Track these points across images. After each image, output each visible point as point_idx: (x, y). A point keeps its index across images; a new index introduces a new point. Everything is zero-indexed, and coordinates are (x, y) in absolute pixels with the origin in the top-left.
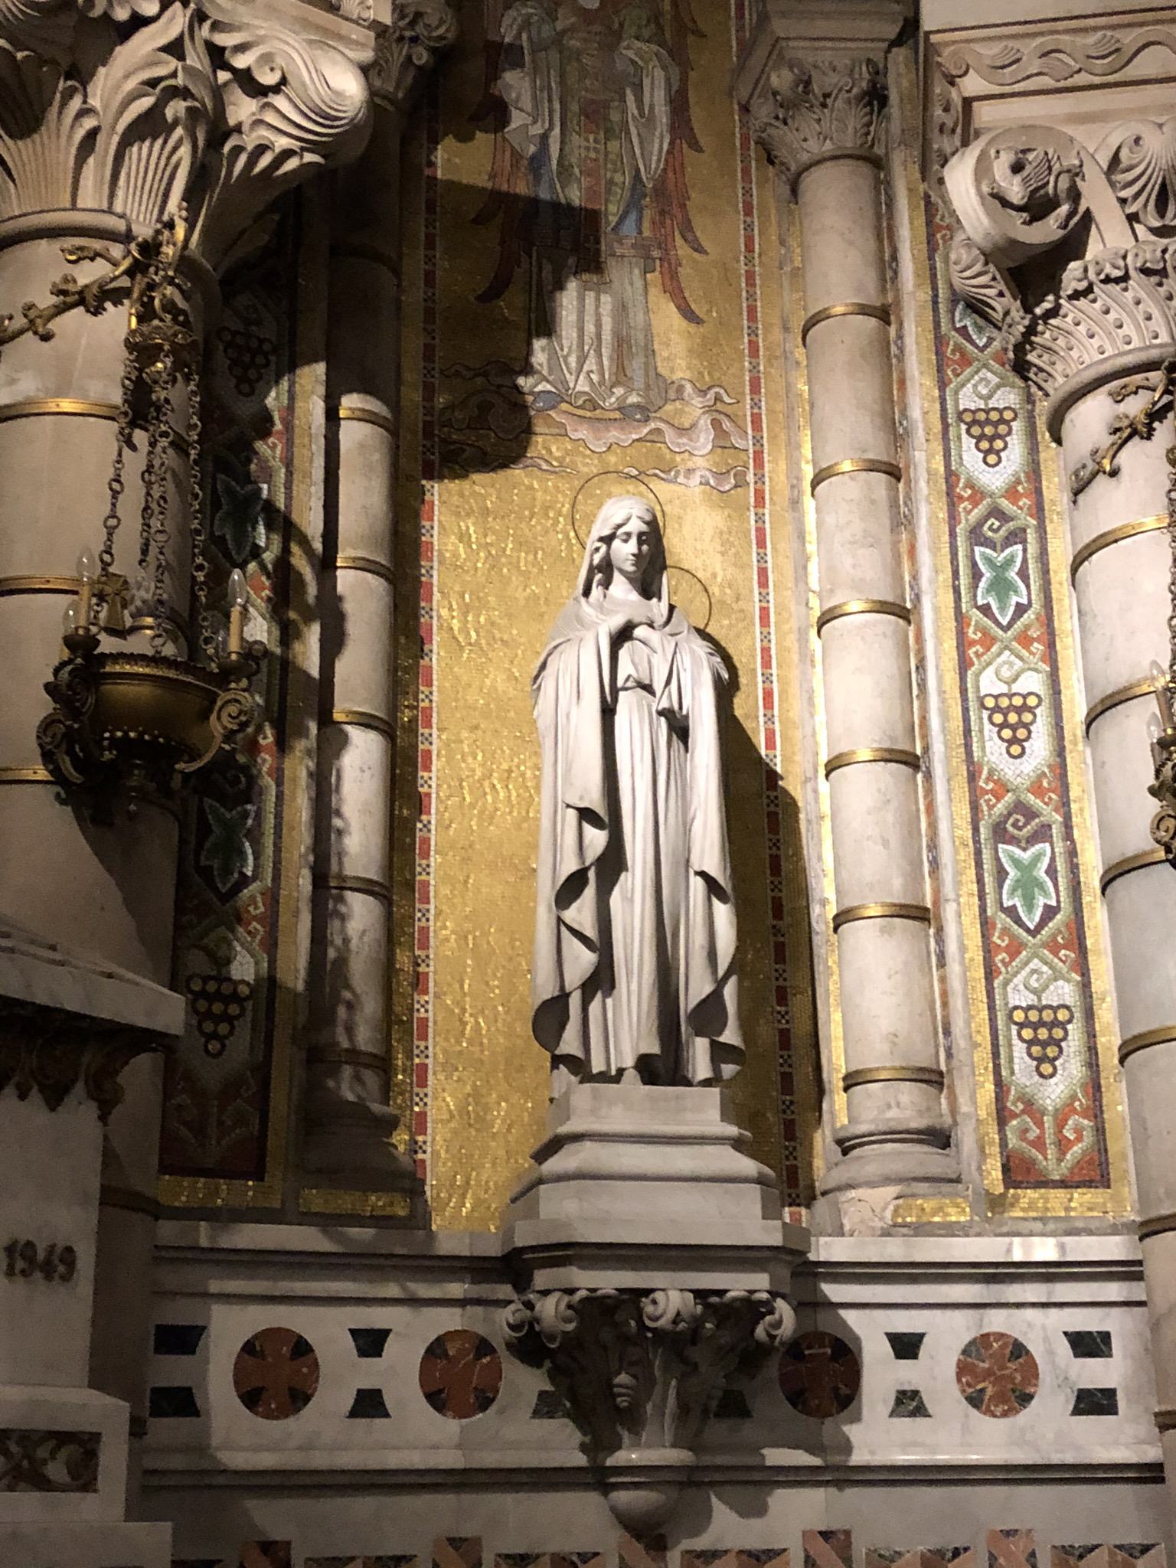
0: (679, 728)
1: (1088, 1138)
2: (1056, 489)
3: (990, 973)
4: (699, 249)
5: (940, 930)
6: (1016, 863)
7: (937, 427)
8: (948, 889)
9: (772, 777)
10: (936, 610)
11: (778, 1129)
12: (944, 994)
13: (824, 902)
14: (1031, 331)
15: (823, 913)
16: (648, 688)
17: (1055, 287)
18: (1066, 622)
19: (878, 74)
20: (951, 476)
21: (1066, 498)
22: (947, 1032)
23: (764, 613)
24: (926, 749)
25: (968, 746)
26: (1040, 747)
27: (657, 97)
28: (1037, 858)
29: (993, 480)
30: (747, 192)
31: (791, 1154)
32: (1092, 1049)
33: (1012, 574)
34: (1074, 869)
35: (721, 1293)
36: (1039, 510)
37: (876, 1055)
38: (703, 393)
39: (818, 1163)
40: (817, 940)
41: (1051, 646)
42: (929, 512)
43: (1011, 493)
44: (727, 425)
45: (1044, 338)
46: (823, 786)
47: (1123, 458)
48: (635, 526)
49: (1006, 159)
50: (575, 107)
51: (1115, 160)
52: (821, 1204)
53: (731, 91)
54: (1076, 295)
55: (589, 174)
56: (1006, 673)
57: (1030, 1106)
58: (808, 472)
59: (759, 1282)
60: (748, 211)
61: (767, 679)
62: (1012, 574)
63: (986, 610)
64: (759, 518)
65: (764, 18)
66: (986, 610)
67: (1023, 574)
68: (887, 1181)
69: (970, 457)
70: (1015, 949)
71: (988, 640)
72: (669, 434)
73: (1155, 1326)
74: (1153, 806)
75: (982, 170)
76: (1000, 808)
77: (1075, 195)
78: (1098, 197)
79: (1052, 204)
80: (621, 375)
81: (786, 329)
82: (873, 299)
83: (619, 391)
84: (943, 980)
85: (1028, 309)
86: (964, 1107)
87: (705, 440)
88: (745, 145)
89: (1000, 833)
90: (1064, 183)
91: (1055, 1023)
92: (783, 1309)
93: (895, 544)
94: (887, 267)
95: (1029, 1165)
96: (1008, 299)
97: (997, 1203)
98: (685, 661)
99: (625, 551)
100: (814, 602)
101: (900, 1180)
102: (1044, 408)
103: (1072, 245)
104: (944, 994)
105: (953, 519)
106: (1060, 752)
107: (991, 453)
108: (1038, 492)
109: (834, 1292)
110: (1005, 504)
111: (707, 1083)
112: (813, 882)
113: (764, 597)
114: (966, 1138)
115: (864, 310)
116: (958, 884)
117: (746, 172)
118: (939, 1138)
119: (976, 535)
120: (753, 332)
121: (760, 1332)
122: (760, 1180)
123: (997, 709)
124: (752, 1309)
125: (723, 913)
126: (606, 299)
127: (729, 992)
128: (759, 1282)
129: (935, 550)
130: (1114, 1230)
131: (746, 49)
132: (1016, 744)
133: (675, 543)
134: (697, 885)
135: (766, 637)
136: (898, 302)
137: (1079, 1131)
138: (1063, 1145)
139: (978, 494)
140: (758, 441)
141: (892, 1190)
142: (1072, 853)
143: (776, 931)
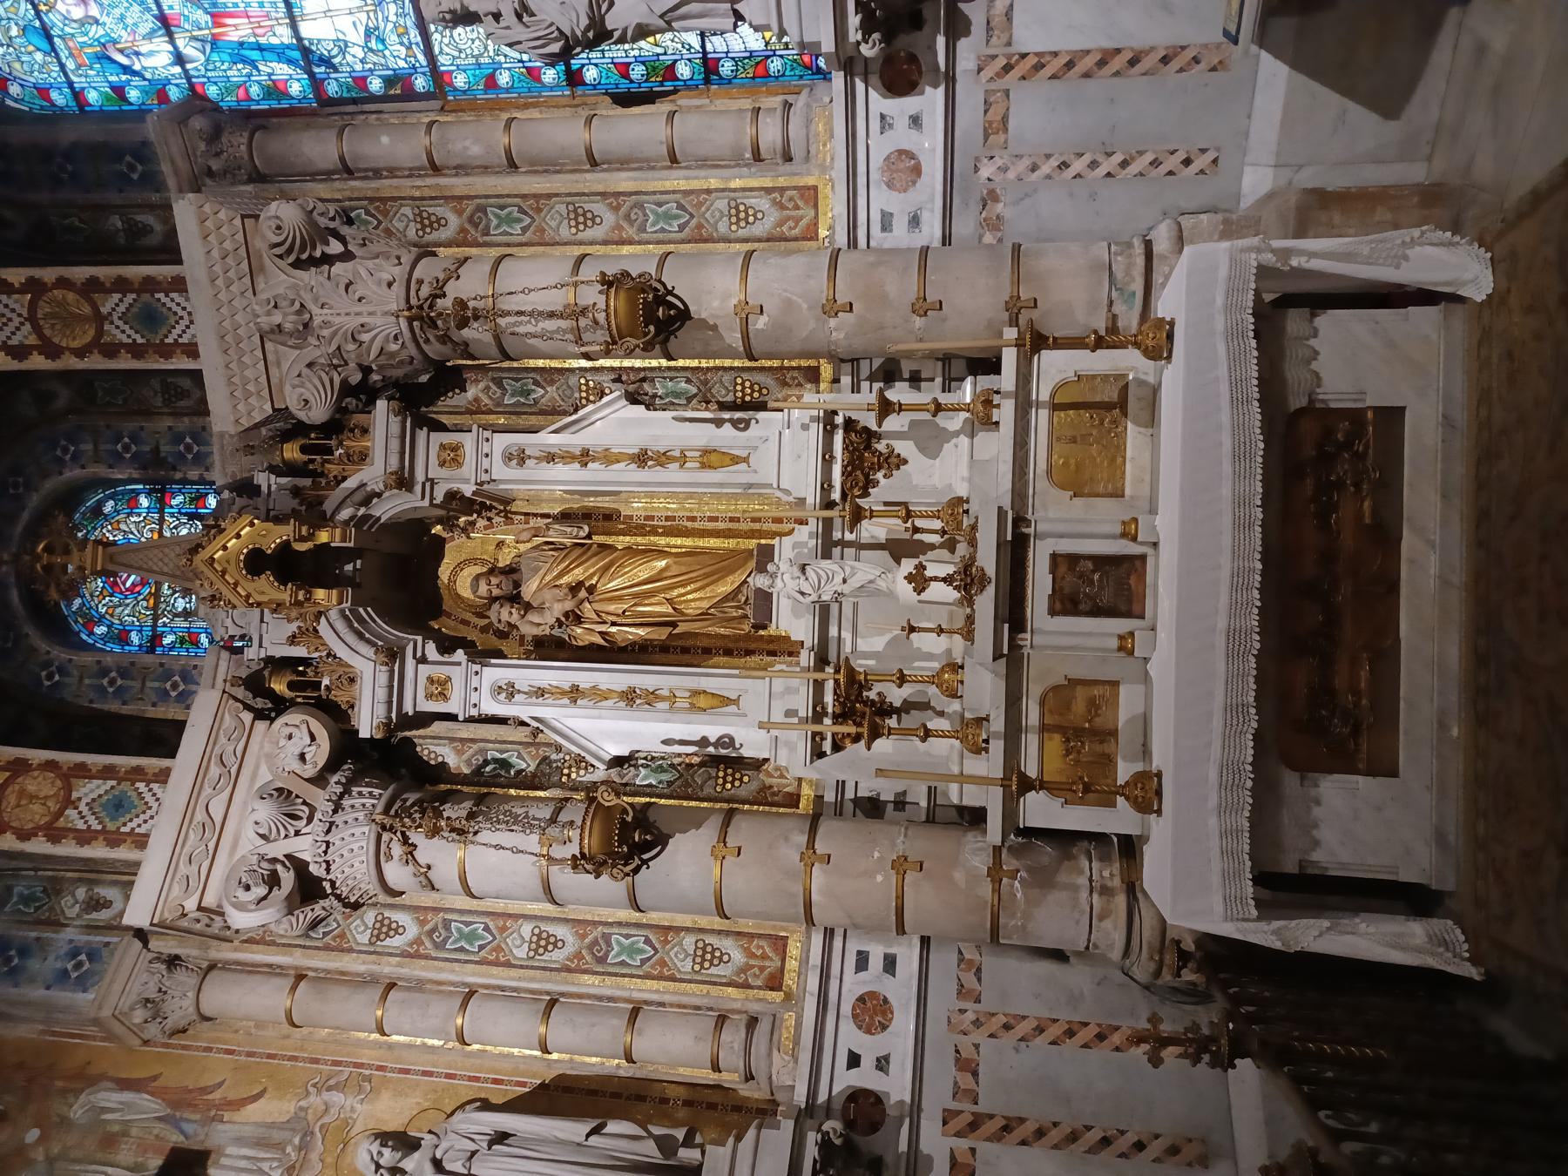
0: (501, 1137)
1: (763, 943)
2: (428, 899)
3: (673, 979)
4: (220, 1084)
5: (646, 1002)
6: (618, 954)
7: (373, 957)
8: (625, 994)
9: (543, 1086)
10: (474, 974)
11: (735, 1116)
12: (679, 1006)
13: (618, 1066)
14: (338, 897)
15: (626, 1070)
16: (474, 1153)
17: (321, 880)
18: (500, 906)
19: (158, 958)
20: (404, 954)
21: (434, 894)
22: (698, 1008)
23: (449, 1076)
24: (548, 993)
25: (551, 970)
26: (561, 931)
27: (110, 1098)
28: (618, 943)
29: (412, 931)
30: (198, 1048)
31: (749, 1110)
32: (720, 932)
33: (466, 930)
34: (628, 925)
35: (815, 1161)
36: (436, 910)
37: (704, 1052)
38: (308, 1094)
39: (756, 1095)
40: (638, 1075)
41: (510, 916)
42: (419, 970)
43: (422, 923)
44: (332, 1082)
45: (344, 891)
46: (555, 1056)
47: (422, 860)
48: (375, 1147)
49: (243, 896)
50: (99, 1155)
51: (263, 836)
52: (779, 1097)
53: (131, 1050)
54: (328, 870)
55: (145, 1151)
56: (518, 942)
57: (744, 969)
58: (375, 1036)
59: (812, 1138)
60: (209, 1049)
61: (486, 1080)
62: (466, 930)
63: (481, 948)
64: (393, 1070)
65: (96, 1022)
66: (481, 948)
67: (467, 924)
68: (770, 1055)
69: (397, 942)
70: (663, 963)
71: (498, 949)
72: (326, 1120)
73: (856, 926)
74: (605, 878)
75: (240, 907)
76: (588, 958)
77: (274, 860)
78: (278, 849)
79: (274, 873)
80: (280, 1146)
81: (288, 1037)
82: (290, 981)
83: (289, 1149)
84: (671, 1005)
85: (326, 896)
86: (737, 1006)
87: (336, 1098)
88: (167, 1046)
89: (602, 960)
90: (265, 865)
91: (704, 949)
92: (826, 1127)
93: (431, 992)
94: (273, 970)
95: (772, 977)
96: (317, 907)
97: (788, 996)
98: (465, 1128)
99: (388, 1157)
100: (450, 1045)
101: (770, 1049)
102: (383, 898)
103: (300, 867)
104: (679, 1006)
105: (427, 957)
106: (566, 921)
107: (398, 930)
108: (426, 908)
109: (822, 1097)
110: (428, 927)
111: (703, 1153)
112: (606, 1072)
113: (439, 1075)
114: (755, 1008)
115: (294, 988)
116: (624, 989)
117: (184, 1047)
118: (753, 1022)
119: (439, 946)
120: (283, 1057)
121: (838, 1142)
122: (759, 1128)
123: (536, 951)
124: (825, 1145)
125: (613, 1127)
126: (230, 1150)
127: (657, 1131)
128: (812, 1138)
129: (441, 970)
130: (809, 938)
131: (110, 1037)
132: (557, 944)
133: (392, 1126)
134: (594, 1140)
135: (462, 1078)
136: (296, 968)
137: (759, 947)
138: (764, 957)
139: (418, 941)
140: (348, 1064)
141: (775, 1052)
142: (620, 924)
143: (628, 1098)
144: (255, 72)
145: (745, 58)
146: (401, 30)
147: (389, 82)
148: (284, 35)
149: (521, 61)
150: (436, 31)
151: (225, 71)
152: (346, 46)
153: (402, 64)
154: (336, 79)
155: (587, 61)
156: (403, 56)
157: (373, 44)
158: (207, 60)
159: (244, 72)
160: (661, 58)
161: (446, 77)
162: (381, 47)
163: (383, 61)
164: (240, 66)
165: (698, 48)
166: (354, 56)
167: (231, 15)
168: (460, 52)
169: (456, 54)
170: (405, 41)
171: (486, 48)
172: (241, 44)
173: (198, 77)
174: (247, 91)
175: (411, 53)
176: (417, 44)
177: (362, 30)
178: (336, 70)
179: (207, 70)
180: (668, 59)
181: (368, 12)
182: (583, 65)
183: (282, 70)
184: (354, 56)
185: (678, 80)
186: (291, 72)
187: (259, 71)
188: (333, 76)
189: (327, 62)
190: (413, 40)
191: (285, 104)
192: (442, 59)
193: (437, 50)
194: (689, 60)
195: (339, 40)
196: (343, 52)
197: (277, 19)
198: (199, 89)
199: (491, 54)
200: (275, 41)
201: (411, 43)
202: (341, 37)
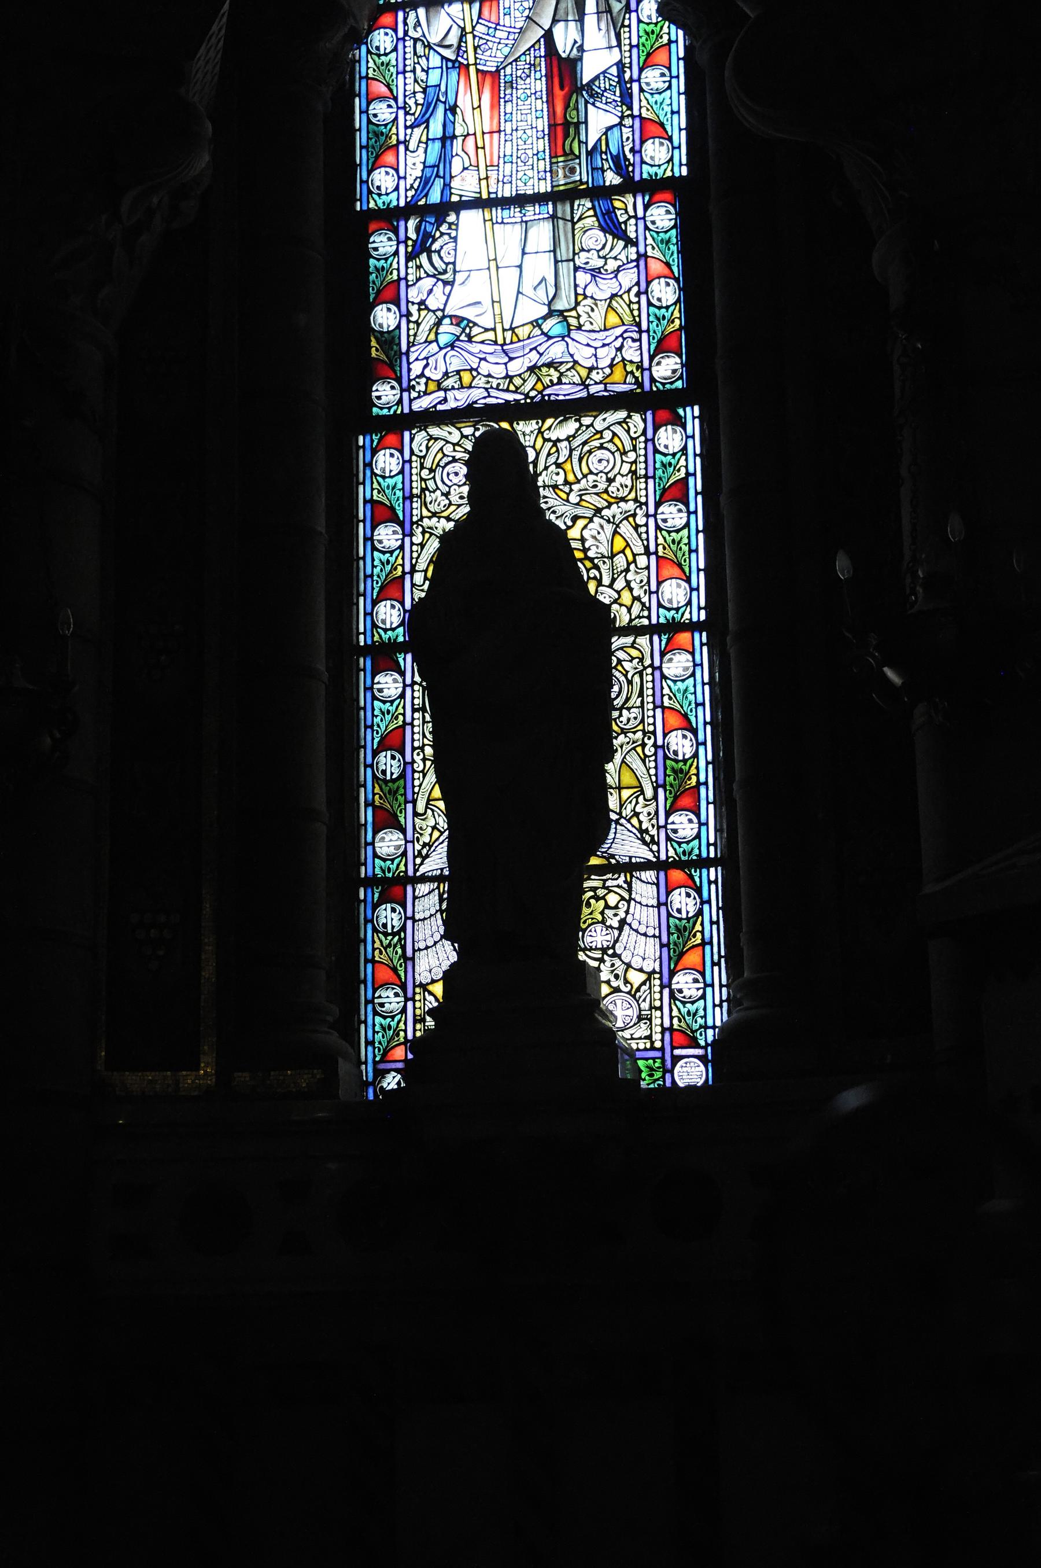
144: (410, 120)
145: (404, 948)
146: (466, 378)
147: (389, 340)
148: (465, 185)
149: (413, 570)
150: (463, 436)
151: (414, 71)
152: (446, 283)
153: (417, 368)
154: (396, 253)
155: (408, 681)
156: (427, 373)
157: (446, 327)
158: (429, 46)
159: (411, 102)
160: (410, 806)
161: (391, 439)
162: (443, 339)
163: (421, 337)
164: (420, 97)
165: (422, 870)
166: (430, 291)
167: (495, 104)
168: (431, 470)
169: (428, 464)
170: (449, 383)
171: (434, 514)
172: (453, 109)
173: (405, 24)
174: (381, 98)
175: (432, 386)
176: (445, 400)
177: (469, 313)
178: (409, 257)
179: (416, 40)
180: (406, 818)
181: (494, 329)
182: (402, 674)
183: (413, 165)
184: (430, 291)
185: (375, 833)
186: (410, 181)
187: (412, 127)
188: (402, 248)
189: (422, 246)
190: (450, 395)
191: (361, 156)
192: (421, 437)
193: (434, 431)
194: (404, 854)
195: (455, 272)
196: (436, 275)
197: (487, 178)
198: (387, 19)
199: (426, 522)
200: (457, 165)
201: (446, 390)
202: (460, 278)
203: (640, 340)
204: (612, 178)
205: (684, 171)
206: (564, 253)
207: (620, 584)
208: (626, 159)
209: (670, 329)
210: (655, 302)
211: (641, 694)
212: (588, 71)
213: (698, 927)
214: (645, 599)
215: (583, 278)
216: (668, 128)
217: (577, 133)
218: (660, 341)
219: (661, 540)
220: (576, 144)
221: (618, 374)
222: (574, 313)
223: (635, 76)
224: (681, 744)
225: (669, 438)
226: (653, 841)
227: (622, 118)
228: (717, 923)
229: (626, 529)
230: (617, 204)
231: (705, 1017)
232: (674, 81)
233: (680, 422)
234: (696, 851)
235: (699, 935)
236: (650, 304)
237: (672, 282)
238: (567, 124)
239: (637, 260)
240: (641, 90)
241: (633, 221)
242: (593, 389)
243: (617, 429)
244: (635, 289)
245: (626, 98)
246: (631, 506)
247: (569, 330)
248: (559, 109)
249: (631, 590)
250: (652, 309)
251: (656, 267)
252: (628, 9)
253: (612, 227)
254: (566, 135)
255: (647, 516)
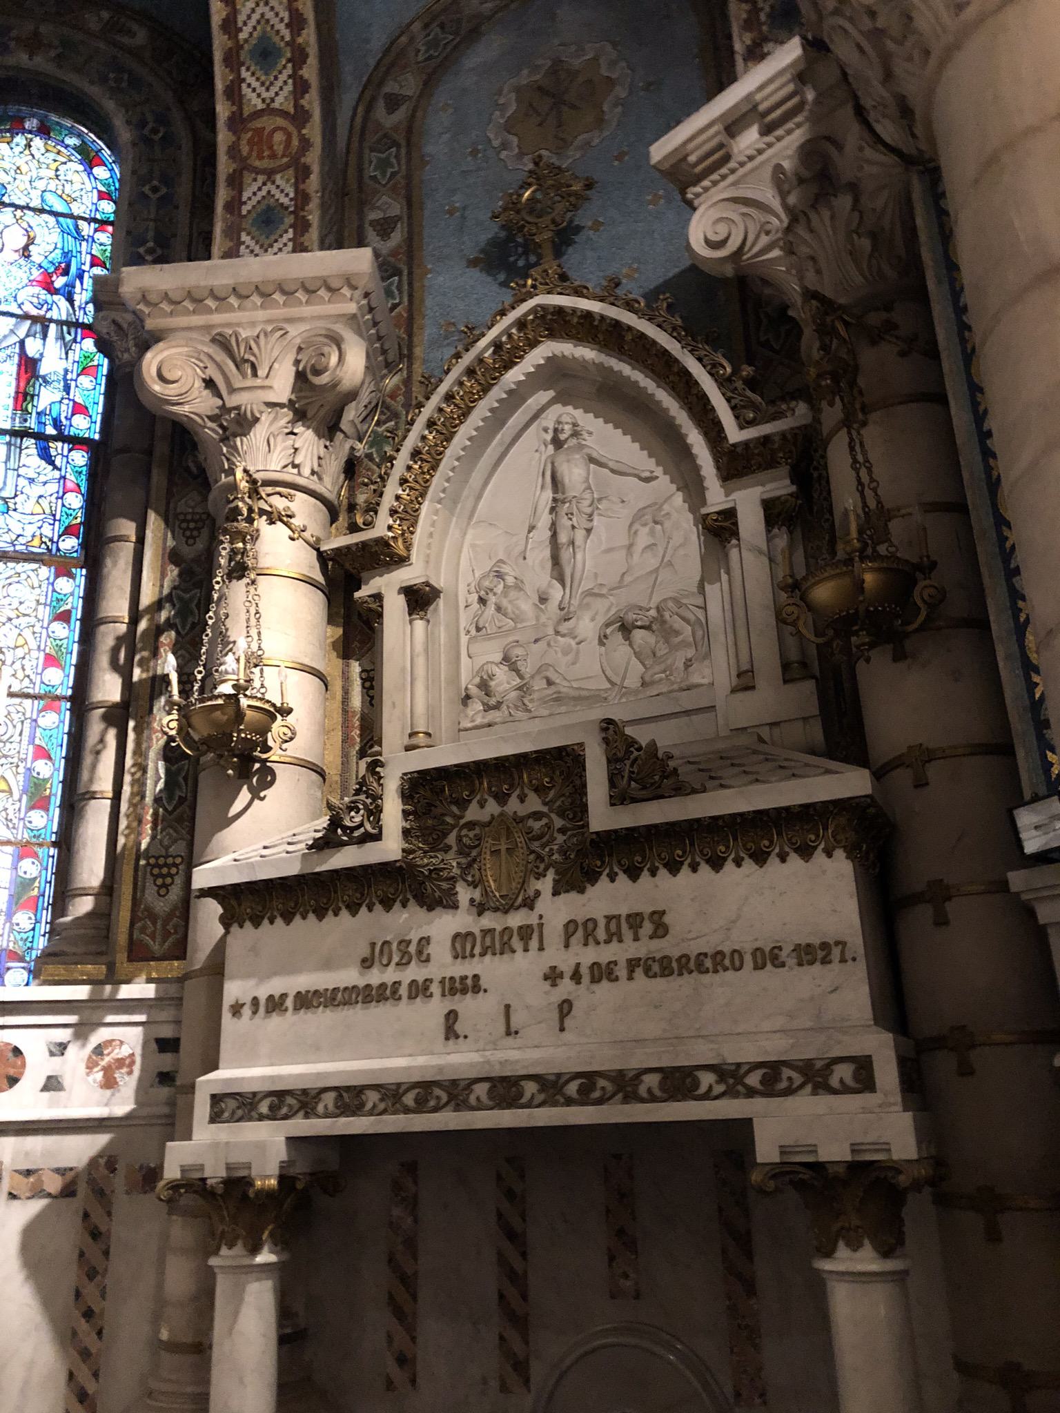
203: (53, 524)
204: (50, 431)
205: (97, 437)
206: (11, 464)
207: (18, 665)
208: (61, 422)
209: (74, 522)
210: (66, 504)
211: (21, 734)
212: (44, 369)
213: (36, 884)
214: (33, 677)
215: (22, 482)
216: (90, 410)
217: (32, 400)
218: (66, 528)
219: (49, 643)
220: (30, 406)
221: (36, 542)
222: (12, 501)
223: (74, 378)
224: (43, 768)
225: (64, 584)
226: (14, 828)
227: (62, 399)
228: (50, 882)
229: (27, 633)
230: (51, 444)
231: (32, 942)
232: (98, 386)
233: (71, 576)
234: (43, 836)
235: (36, 890)
236: (63, 505)
237: (80, 496)
238: (26, 394)
239: (60, 479)
240: (77, 386)
241: (60, 456)
242: (18, 548)
243: (32, 574)
244: (56, 495)
245: (67, 389)
246: (32, 620)
247: (8, 510)
248: (22, 384)
249: (24, 670)
250: (64, 509)
251: (70, 485)
252: (75, 341)
253: (46, 456)
254: (25, 400)
255: (42, 627)
